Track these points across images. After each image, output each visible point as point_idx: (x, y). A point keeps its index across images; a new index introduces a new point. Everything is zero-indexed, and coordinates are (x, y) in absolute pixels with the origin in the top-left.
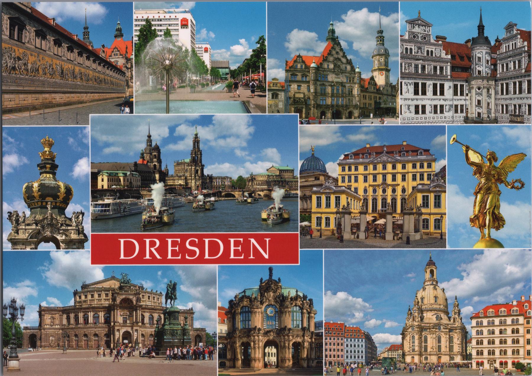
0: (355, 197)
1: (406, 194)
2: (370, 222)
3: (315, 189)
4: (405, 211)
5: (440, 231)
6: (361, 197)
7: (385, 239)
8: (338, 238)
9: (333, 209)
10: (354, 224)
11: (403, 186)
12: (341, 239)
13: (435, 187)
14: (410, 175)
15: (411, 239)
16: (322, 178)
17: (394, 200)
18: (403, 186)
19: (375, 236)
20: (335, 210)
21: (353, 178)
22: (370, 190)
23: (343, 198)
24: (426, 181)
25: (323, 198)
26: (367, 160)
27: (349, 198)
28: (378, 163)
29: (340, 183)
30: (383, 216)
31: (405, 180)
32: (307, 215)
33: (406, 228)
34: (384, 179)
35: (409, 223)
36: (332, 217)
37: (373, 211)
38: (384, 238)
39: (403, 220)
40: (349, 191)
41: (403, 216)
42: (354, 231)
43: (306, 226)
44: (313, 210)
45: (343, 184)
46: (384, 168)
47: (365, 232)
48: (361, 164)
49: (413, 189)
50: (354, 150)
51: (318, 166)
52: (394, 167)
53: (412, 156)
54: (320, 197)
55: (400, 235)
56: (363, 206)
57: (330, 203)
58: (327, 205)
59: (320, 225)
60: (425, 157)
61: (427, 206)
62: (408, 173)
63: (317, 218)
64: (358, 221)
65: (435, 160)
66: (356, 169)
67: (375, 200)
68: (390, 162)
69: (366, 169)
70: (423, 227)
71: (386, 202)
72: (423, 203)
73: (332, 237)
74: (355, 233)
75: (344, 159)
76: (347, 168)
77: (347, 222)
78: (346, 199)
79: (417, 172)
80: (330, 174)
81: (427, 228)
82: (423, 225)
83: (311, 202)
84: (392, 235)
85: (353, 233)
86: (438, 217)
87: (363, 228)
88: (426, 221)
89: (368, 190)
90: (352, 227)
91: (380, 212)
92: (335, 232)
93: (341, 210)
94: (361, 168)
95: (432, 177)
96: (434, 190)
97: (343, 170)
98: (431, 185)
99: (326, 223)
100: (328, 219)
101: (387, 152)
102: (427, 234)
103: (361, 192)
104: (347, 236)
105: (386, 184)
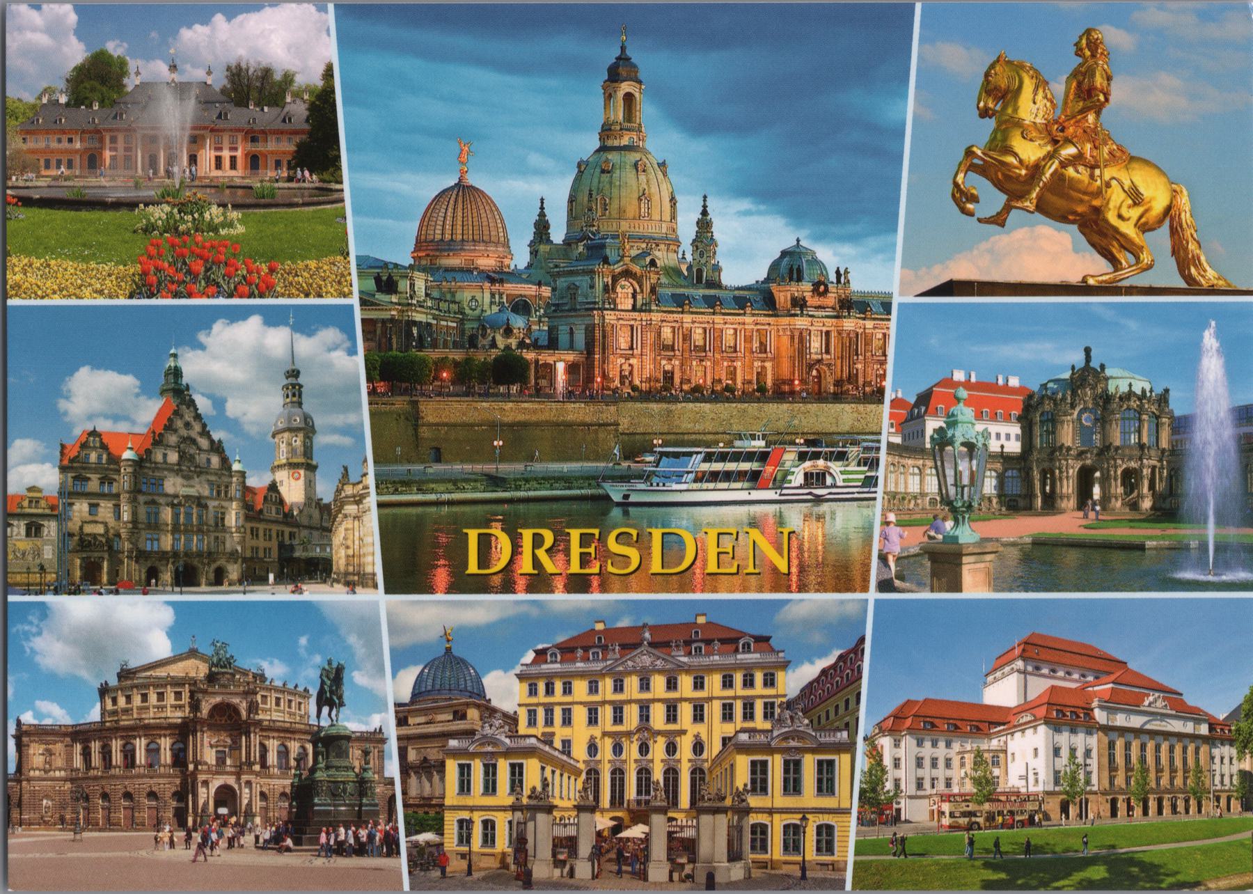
0: (563, 767)
1: (705, 756)
2: (606, 834)
3: (453, 743)
4: (701, 804)
5: (799, 858)
6: (581, 766)
7: (646, 879)
8: (518, 878)
9: (503, 796)
10: (561, 839)
11: (697, 736)
12: (526, 879)
13: (786, 737)
14: (717, 707)
15: (719, 879)
16: (473, 714)
17: (672, 774)
18: (697, 736)
19: (619, 872)
20: (510, 801)
21: (558, 713)
22: (607, 746)
23: (532, 768)
24: (760, 722)
25: (478, 768)
26: (598, 666)
27: (548, 769)
28: (630, 673)
29: (523, 728)
30: (640, 816)
31: (702, 719)
32: (432, 813)
33: (704, 849)
34: (645, 716)
35: (713, 835)
36: (502, 822)
37: (612, 802)
38: (643, 875)
39: (697, 828)
40: (547, 748)
41: (697, 818)
42: (561, 857)
43: (428, 843)
44: (448, 802)
45: (532, 731)
46: (645, 685)
47: (591, 859)
48: (581, 675)
49: (724, 744)
50: (561, 638)
51: (462, 682)
52: (672, 685)
53: (720, 653)
54: (469, 766)
55: (688, 869)
56: (585, 789)
57: (494, 782)
58: (486, 788)
59: (468, 842)
60: (758, 655)
61: (764, 790)
62: (710, 699)
63: (461, 822)
64: (571, 831)
65: (785, 665)
66: (567, 690)
67: (618, 775)
68: (660, 672)
69: (593, 689)
70: (753, 848)
71: (648, 779)
72: (753, 781)
73: (499, 875)
74: (563, 863)
75: (535, 662)
76: (541, 687)
77: (542, 831)
78: (539, 771)
79: (735, 698)
80: (494, 703)
81: (764, 849)
82: (753, 841)
83: (442, 779)
84: (667, 867)
85: (558, 863)
86: (795, 819)
87: (585, 848)
88: (760, 831)
89: (599, 746)
90: (555, 846)
91: (634, 806)
92: (510, 860)
93: (525, 801)
94: (580, 688)
95: (777, 711)
96: (784, 745)
97: (533, 691)
98: (776, 733)
99: (485, 836)
100: (489, 825)
101: (651, 644)
102: (763, 865)
103: (580, 752)
104: (541, 869)
105: (648, 729)
